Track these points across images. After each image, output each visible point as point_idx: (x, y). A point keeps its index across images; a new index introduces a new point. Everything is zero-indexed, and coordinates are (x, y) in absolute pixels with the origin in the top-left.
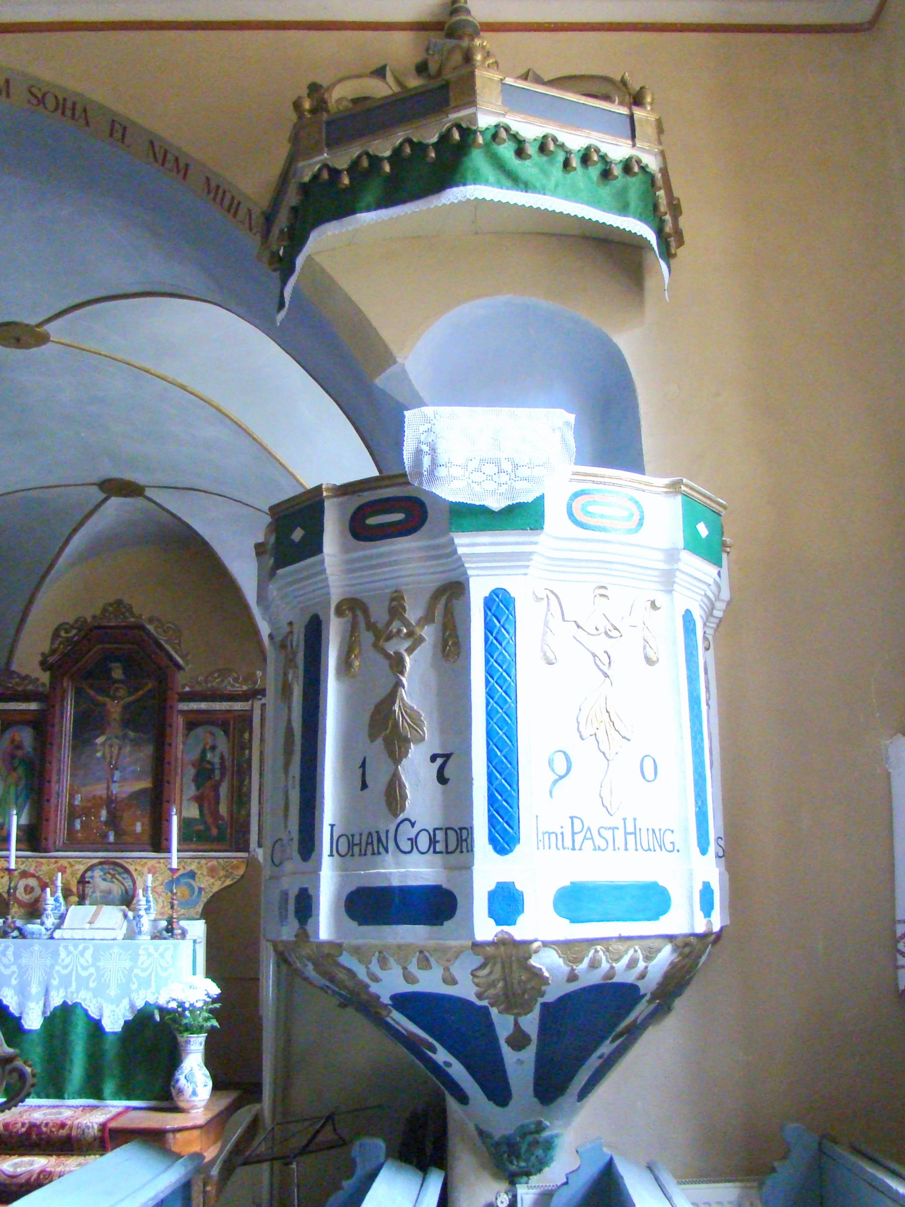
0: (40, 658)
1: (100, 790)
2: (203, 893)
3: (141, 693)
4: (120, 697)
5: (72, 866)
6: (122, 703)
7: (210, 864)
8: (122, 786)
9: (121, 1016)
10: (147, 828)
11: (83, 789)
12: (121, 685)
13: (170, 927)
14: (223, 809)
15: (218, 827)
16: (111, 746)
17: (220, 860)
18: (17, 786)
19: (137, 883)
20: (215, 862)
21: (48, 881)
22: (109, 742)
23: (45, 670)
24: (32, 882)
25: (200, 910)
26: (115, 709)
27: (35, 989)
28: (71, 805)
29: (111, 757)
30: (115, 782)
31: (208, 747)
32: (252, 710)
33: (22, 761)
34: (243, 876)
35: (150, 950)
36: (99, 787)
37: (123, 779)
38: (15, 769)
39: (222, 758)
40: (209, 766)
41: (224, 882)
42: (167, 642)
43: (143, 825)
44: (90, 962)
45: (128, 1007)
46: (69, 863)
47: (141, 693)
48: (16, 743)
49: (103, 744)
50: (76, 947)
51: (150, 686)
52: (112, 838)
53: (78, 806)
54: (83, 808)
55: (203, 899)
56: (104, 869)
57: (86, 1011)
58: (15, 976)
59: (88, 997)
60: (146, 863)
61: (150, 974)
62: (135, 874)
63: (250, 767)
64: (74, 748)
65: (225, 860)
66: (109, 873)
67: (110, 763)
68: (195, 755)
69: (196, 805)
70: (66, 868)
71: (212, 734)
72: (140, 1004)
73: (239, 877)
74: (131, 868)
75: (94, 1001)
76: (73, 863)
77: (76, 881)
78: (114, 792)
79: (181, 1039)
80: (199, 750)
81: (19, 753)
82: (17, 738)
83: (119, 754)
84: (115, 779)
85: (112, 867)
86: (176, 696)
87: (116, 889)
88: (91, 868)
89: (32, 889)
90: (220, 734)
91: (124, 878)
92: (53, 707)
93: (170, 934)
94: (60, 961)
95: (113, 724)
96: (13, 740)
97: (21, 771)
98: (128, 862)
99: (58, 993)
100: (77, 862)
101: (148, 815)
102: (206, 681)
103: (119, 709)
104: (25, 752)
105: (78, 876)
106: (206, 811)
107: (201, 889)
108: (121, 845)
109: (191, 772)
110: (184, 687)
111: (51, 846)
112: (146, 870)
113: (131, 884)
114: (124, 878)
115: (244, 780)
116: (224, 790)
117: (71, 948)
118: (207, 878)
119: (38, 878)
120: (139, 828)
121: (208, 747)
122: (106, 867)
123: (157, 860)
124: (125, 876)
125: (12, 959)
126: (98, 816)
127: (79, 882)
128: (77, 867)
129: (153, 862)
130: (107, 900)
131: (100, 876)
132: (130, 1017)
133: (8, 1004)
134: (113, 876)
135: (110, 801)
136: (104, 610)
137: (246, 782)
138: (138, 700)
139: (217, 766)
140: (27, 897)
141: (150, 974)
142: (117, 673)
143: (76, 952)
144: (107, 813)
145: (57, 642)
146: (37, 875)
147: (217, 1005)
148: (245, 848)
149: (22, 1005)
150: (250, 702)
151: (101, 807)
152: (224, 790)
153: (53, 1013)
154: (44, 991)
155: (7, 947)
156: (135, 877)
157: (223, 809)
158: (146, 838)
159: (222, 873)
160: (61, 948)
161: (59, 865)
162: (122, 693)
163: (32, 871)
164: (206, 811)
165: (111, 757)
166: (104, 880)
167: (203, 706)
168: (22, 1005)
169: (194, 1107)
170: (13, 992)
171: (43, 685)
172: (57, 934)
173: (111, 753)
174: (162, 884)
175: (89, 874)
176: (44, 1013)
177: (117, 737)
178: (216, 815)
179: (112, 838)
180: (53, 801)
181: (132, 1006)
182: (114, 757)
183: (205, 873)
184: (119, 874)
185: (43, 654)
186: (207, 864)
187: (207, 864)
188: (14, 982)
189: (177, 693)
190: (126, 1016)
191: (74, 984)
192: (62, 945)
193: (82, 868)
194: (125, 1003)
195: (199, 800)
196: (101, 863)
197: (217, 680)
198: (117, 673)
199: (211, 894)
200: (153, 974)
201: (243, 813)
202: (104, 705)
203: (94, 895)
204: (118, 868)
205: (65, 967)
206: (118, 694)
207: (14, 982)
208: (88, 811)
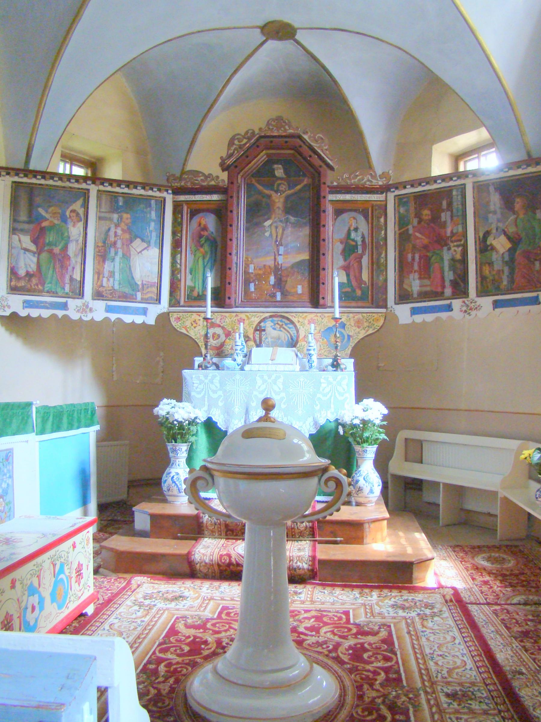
0: (220, 161)
1: (269, 261)
2: (351, 339)
3: (299, 187)
4: (282, 190)
5: (248, 318)
6: (284, 195)
7: (356, 317)
8: (287, 258)
10: (307, 290)
11: (255, 261)
12: (283, 182)
13: (335, 363)
14: (365, 276)
15: (361, 288)
16: (276, 227)
17: (363, 314)
18: (204, 258)
19: (300, 331)
20: (360, 316)
21: (230, 330)
22: (275, 224)
23: (223, 170)
24: (219, 331)
25: (349, 352)
26: (278, 200)
27: (238, 409)
28: (246, 273)
30: (281, 255)
31: (352, 228)
32: (386, 200)
33: (207, 239)
34: (382, 327)
36: (268, 258)
37: (286, 253)
38: (202, 246)
39: (363, 237)
40: (354, 243)
41: (368, 331)
42: (319, 148)
43: (303, 288)
44: (282, 389)
45: (312, 424)
46: (248, 317)
47: (299, 187)
48: (202, 226)
49: (271, 225)
50: (270, 377)
51: (305, 182)
52: (279, 297)
54: (256, 275)
55: (351, 344)
56: (275, 321)
58: (221, 399)
60: (306, 316)
62: (297, 324)
63: (386, 244)
64: (247, 229)
65: (368, 314)
66: (278, 324)
67: (277, 241)
68: (343, 235)
69: (344, 273)
70: (244, 320)
71: (354, 218)
72: (322, 422)
73: (378, 328)
74: (295, 320)
76: (250, 316)
77: (252, 330)
78: (280, 263)
79: (357, 448)
80: (346, 229)
81: (205, 233)
82: (203, 222)
83: (283, 234)
85: (280, 319)
86: (328, 189)
87: (284, 336)
88: (263, 320)
89: (219, 336)
90: (361, 218)
91: (290, 328)
92: (232, 197)
93: (334, 369)
94: (257, 388)
95: (277, 210)
96: (200, 224)
97: (206, 248)
98: (292, 316)
100: (253, 315)
101: (307, 280)
102: (349, 178)
103: (282, 200)
104: (209, 232)
105: (254, 326)
106: (352, 277)
107: (349, 337)
108: (286, 302)
109: (339, 247)
110: (332, 183)
111: (233, 303)
112: (306, 322)
113: (295, 332)
114: (290, 328)
115: (381, 254)
116: (365, 261)
117: (266, 377)
118: (354, 328)
119: (223, 328)
120: (300, 290)
121: (352, 228)
122: (276, 319)
123: (315, 314)
124: (291, 326)
125: (218, 385)
126: (267, 281)
127: (256, 330)
128: (253, 319)
129: (312, 315)
130: (276, 343)
131: (271, 326)
132: (314, 431)
133: (216, 421)
134: (281, 326)
135: (277, 270)
136: (268, 124)
137: (383, 255)
138: (296, 193)
139: (360, 243)
140: (215, 342)
142: (279, 172)
144: (275, 278)
145: (233, 148)
146: (222, 325)
147: (385, 423)
148: (386, 307)
149: (227, 422)
150: (384, 194)
151: (271, 273)
152: (365, 261)
154: (245, 411)
155: (214, 377)
156: (298, 327)
157: (365, 276)
158: (306, 298)
159: (366, 324)
160: (258, 378)
161: (239, 318)
162: (283, 188)
163: (218, 322)
164: (352, 277)
166: (274, 329)
167: (348, 197)
168: (227, 422)
169: (370, 502)
170: (220, 411)
171: (223, 181)
172: (247, 367)
173: (277, 233)
174: (319, 333)
175: (262, 324)
177: (281, 221)
178: (359, 279)
179: (279, 297)
180: (234, 269)
181: (316, 423)
182: (279, 237)
183: (353, 325)
184: (286, 324)
185: (221, 158)
186: (354, 317)
187: (354, 317)
188: (220, 404)
189: (328, 186)
190: (311, 431)
192: (258, 375)
193: (256, 320)
194: (310, 420)
195: (346, 269)
196: (271, 317)
197: (358, 178)
198: (279, 172)
199: (357, 340)
200: (332, 398)
201: (381, 278)
202: (269, 197)
203: (267, 340)
204: (284, 320)
206: (281, 189)
207: (220, 404)
208: (260, 278)
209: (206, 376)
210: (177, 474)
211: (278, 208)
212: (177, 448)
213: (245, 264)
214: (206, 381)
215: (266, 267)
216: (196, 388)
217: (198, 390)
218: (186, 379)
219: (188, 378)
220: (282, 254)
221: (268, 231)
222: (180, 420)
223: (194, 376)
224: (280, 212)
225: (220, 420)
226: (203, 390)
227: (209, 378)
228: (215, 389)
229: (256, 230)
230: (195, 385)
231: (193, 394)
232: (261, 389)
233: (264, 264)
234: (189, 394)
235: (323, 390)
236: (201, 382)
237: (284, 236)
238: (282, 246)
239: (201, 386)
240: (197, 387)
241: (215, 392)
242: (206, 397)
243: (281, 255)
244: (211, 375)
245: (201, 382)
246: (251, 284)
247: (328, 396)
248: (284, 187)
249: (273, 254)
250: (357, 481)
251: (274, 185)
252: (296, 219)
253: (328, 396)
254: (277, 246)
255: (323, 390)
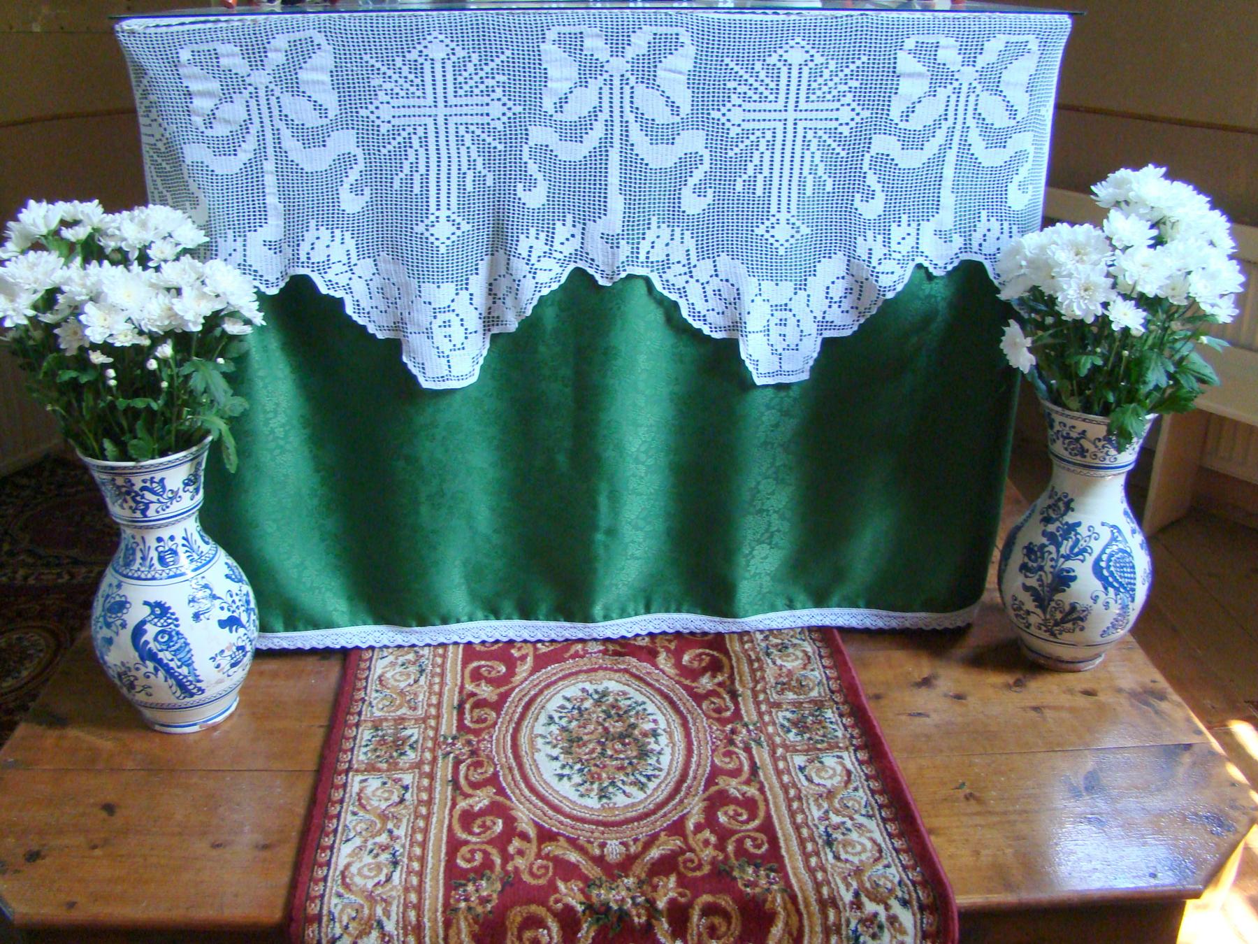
9: (810, 327)
35: (942, 55)
44: (686, 109)
57: (670, 310)
58: (354, 175)
59: (678, 254)
61: (940, 158)
75: (704, 269)
94: (548, 104)
99: (550, 241)
125: (330, 100)
132: (845, 324)
141: (940, 158)
143: (618, 66)
153: (530, 325)
155: (300, 53)
160: (550, 51)
170: (351, 244)
176: (490, 320)
181: (858, 285)
188: (351, 203)
190: (831, 325)
191: (616, 203)
192: (551, 35)
194: (831, 270)
200: (951, 156)
205: (575, 132)
209: (256, 53)
210: (161, 610)
212: (138, 483)
214: (261, 79)
216: (211, 119)
217: (220, 130)
218: (142, 72)
219: (154, 66)
222: (125, 338)
223: (185, 55)
225: (359, 287)
226: (245, 127)
227: (276, 58)
228: (311, 119)
230: (202, 104)
231: (194, 153)
232: (572, 112)
234: (173, 155)
235: (906, 117)
236: (231, 86)
239: (235, 111)
240: (211, 119)
241: (313, 138)
242: (269, 166)
244: (281, 42)
245: (231, 86)
247: (932, 147)
250: (1064, 580)
253: (932, 147)
255: (906, 117)
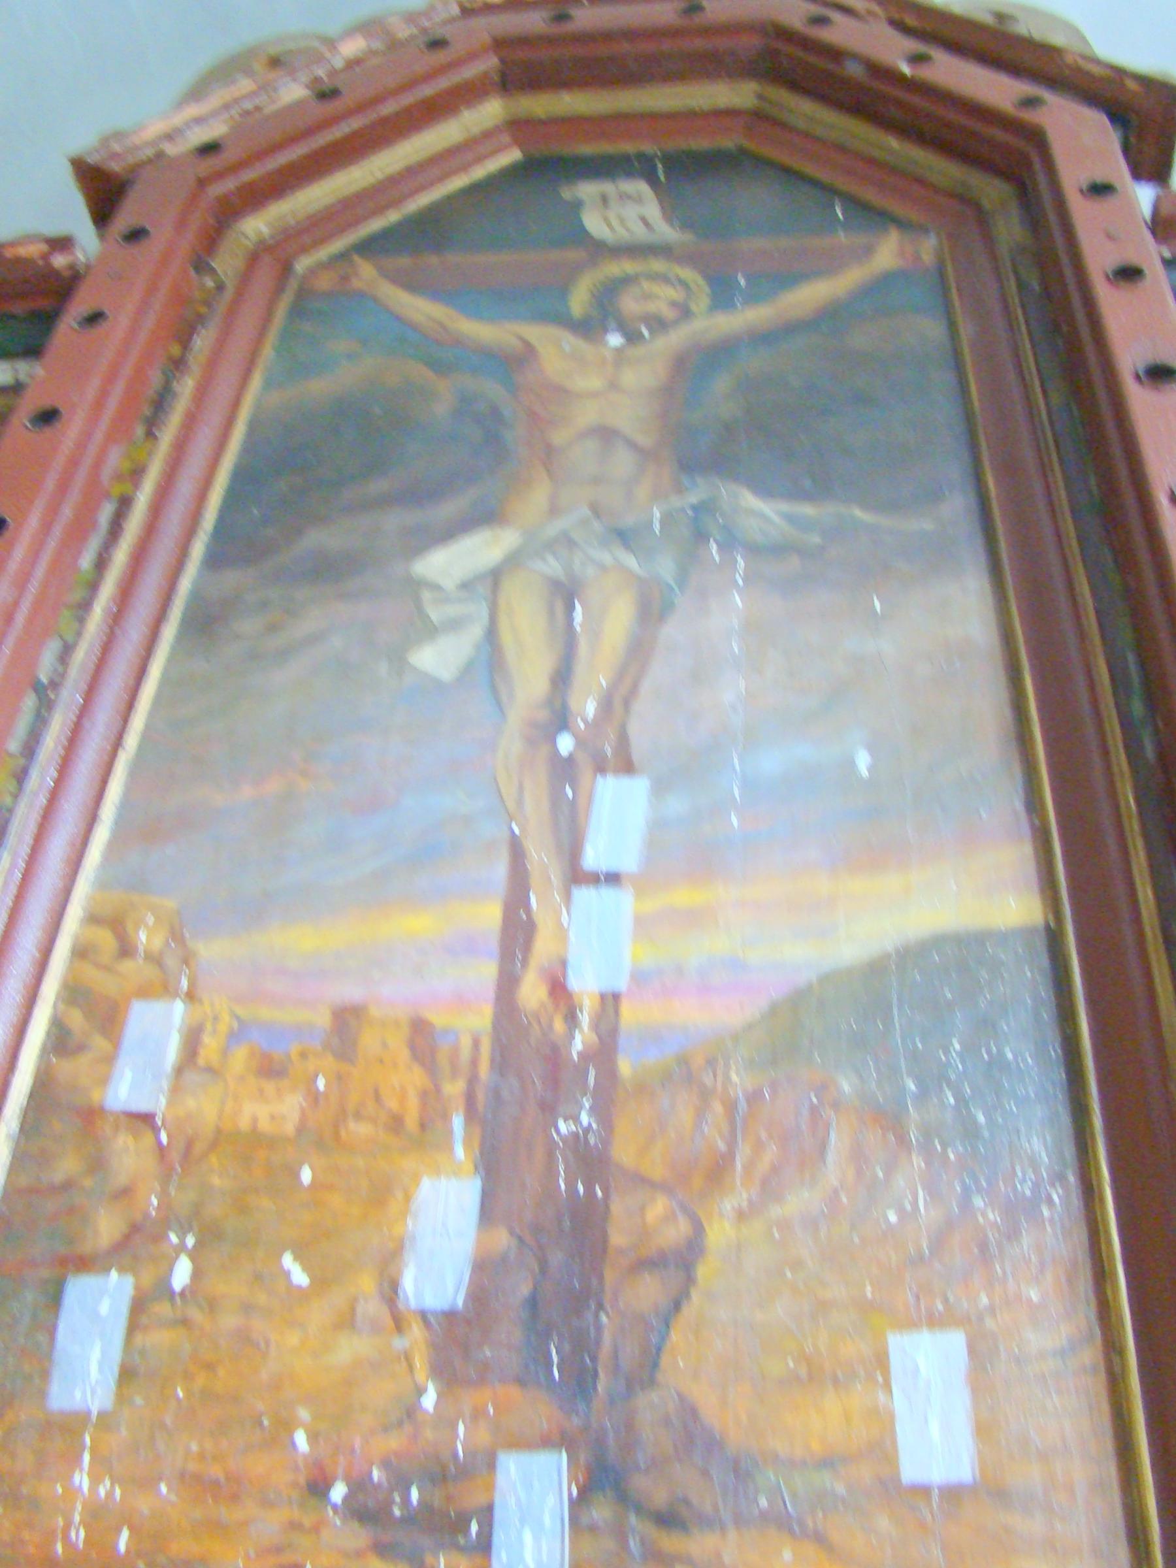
12: (658, 265)
29: (562, 678)
30: (613, 879)
49: (495, 577)
53: (146, 1119)
84: (593, 858)
144: (487, 1212)
165: (562, 678)
177: (624, 537)
211: (606, 435)
213: (73, 993)
215: (369, 1041)
220: (628, 861)
221: (454, 625)
224: (623, 462)
229: (310, 622)
233: (349, 991)
237: (658, 674)
238: (627, 767)
243: (613, 879)
246: (78, 1288)
248: (672, 293)
249: (500, 870)
251: (564, 292)
252: (807, 510)
254: (564, 769)
